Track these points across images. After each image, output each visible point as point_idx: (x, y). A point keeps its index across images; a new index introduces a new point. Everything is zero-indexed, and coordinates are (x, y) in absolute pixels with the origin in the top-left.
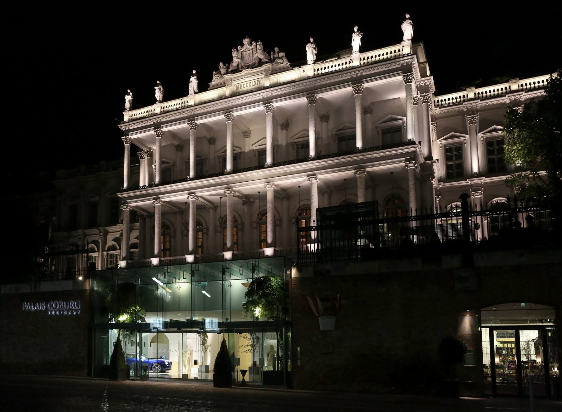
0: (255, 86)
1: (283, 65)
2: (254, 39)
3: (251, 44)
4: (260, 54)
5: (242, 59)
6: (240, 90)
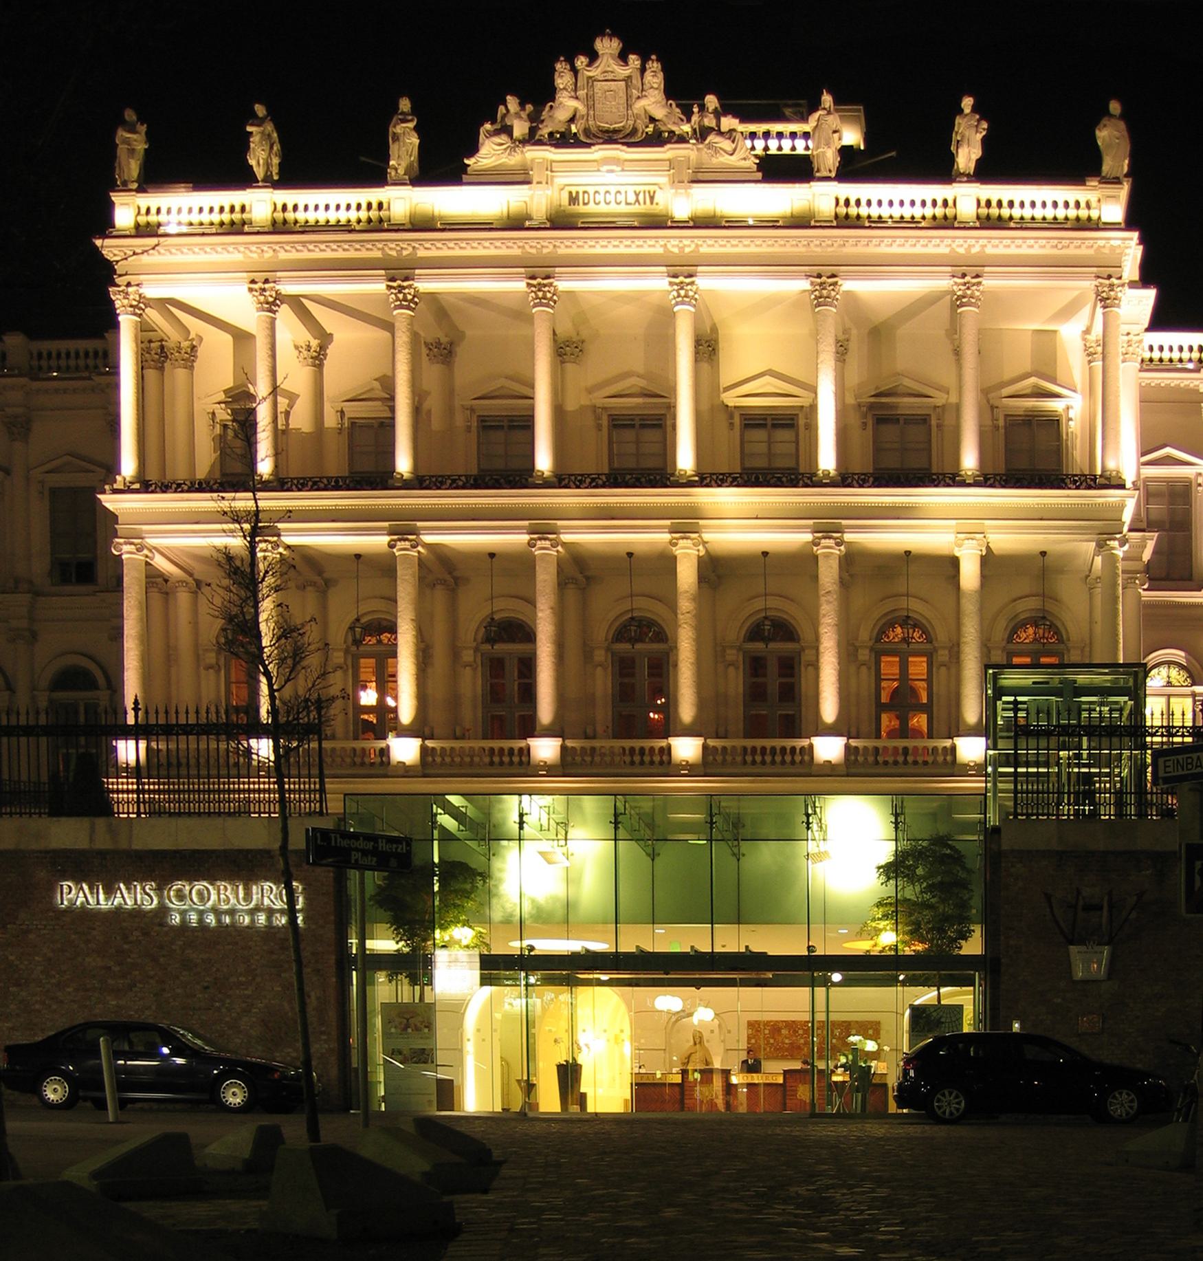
0: (636, 209)
1: (733, 161)
3: (623, 57)
4: (653, 102)
5: (590, 101)
6: (581, 208)
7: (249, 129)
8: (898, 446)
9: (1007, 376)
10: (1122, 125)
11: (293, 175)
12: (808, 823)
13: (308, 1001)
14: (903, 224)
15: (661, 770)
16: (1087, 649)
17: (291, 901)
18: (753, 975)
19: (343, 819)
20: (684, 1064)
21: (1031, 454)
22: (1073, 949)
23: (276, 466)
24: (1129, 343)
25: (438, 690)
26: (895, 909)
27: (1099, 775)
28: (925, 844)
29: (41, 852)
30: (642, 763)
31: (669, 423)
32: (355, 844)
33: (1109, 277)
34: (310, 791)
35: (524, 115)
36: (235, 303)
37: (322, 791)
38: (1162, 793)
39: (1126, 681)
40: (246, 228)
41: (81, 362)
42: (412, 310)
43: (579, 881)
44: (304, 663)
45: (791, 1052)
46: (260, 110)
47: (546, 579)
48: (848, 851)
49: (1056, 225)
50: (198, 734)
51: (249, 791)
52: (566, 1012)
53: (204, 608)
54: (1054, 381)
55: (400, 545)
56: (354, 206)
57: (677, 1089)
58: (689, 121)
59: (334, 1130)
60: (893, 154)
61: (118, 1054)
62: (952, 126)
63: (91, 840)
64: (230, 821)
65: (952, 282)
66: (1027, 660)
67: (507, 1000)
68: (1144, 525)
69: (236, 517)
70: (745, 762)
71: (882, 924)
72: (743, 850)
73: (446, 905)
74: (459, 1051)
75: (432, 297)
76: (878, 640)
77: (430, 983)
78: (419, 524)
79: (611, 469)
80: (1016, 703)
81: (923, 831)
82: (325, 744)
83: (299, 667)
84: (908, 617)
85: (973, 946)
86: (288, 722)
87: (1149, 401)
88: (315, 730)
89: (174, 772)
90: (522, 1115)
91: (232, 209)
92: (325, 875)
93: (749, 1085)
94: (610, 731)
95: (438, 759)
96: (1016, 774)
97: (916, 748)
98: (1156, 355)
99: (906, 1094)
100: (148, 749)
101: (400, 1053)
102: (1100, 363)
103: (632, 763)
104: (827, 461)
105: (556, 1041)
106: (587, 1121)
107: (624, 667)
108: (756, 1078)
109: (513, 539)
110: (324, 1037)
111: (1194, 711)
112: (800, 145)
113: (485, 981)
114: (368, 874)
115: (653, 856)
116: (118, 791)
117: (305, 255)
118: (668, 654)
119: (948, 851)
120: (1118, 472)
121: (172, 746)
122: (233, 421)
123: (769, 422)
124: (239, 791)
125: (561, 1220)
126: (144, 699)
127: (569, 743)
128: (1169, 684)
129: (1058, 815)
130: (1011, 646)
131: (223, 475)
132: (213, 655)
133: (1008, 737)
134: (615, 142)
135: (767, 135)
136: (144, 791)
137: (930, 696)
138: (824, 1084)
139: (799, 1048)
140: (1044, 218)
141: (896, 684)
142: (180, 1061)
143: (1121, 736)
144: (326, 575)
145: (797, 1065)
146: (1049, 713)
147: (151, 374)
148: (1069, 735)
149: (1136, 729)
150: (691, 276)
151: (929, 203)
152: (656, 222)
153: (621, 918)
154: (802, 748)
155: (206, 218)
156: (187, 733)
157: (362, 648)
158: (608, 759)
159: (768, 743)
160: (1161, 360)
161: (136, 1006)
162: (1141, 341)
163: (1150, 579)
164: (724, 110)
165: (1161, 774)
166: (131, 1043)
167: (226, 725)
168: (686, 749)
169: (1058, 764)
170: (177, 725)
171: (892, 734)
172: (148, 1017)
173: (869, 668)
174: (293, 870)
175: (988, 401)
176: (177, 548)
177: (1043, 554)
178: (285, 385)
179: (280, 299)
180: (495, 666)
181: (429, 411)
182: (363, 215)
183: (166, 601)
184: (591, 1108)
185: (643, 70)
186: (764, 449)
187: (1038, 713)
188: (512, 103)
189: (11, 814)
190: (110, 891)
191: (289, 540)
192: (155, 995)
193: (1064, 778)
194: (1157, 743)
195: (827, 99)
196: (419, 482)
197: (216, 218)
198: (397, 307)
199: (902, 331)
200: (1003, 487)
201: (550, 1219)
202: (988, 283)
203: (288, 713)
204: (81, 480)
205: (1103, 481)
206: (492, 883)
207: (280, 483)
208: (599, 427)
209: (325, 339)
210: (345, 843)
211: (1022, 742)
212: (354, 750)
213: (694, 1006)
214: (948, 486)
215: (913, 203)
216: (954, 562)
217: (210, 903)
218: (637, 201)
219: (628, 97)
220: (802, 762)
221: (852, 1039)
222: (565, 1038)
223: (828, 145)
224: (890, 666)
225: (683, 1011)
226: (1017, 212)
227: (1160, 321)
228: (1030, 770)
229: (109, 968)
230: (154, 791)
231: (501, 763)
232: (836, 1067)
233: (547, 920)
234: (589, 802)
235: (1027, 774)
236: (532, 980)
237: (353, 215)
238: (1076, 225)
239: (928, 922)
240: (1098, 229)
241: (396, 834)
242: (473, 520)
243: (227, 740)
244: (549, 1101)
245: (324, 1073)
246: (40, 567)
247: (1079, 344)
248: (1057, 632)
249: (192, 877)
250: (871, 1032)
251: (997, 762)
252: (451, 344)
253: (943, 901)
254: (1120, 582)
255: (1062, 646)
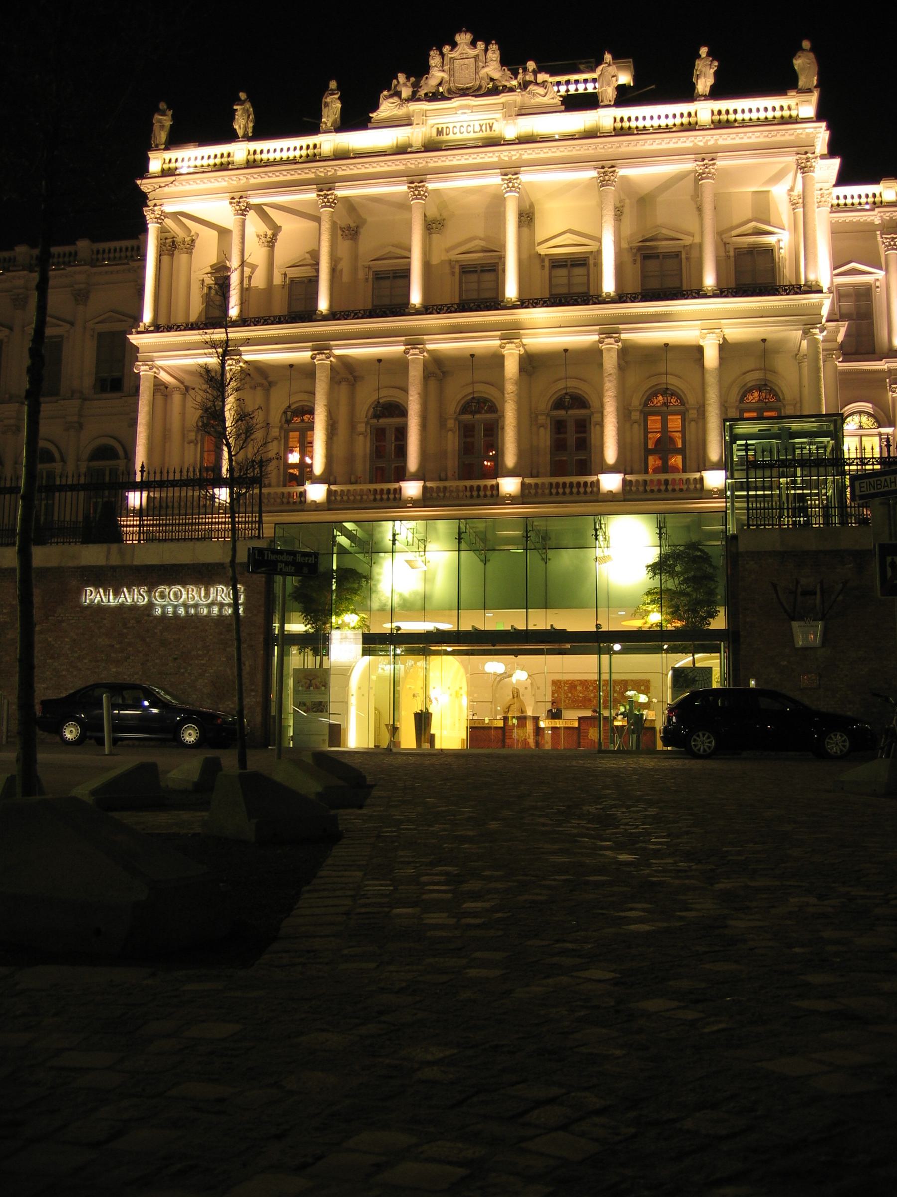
1: (545, 100)
2: (481, 36)
3: (473, 44)
4: (493, 69)
6: (444, 137)
7: (235, 107)
8: (660, 273)
9: (735, 222)
10: (811, 55)
11: (261, 132)
12: (596, 535)
13: (243, 668)
14: (659, 130)
15: (492, 501)
16: (799, 405)
17: (236, 598)
18: (556, 646)
19: (273, 540)
20: (505, 712)
21: (753, 272)
22: (795, 624)
23: (241, 311)
24: (822, 195)
25: (340, 451)
26: (660, 596)
27: (810, 495)
28: (681, 548)
29: (74, 568)
30: (479, 496)
31: (500, 268)
32: (280, 557)
33: (806, 153)
34: (252, 522)
35: (409, 84)
36: (221, 212)
37: (260, 522)
38: (859, 507)
39: (828, 427)
40: (230, 166)
41: (123, 254)
42: (333, 208)
43: (432, 580)
44: (253, 437)
45: (583, 703)
46: (243, 96)
47: (415, 375)
48: (625, 555)
49: (767, 122)
50: (181, 486)
51: (212, 523)
52: (421, 674)
53: (190, 404)
54: (768, 223)
55: (319, 357)
56: (298, 148)
57: (500, 731)
58: (516, 78)
59: (257, 761)
60: (653, 87)
61: (114, 706)
62: (693, 66)
63: (107, 559)
64: (198, 544)
65: (695, 164)
66: (755, 415)
67: (381, 666)
68: (837, 317)
69: (213, 345)
70: (551, 494)
71: (650, 608)
72: (549, 556)
73: (340, 599)
74: (346, 703)
75: (346, 199)
76: (646, 405)
77: (328, 654)
78: (332, 343)
79: (460, 300)
80: (747, 445)
81: (680, 539)
82: (264, 490)
83: (249, 440)
84: (667, 389)
85: (719, 623)
86: (240, 477)
87: (837, 233)
88: (257, 481)
89: (163, 512)
90: (389, 750)
91: (222, 156)
92: (259, 579)
93: (553, 728)
94: (457, 475)
95: (339, 498)
96: (748, 496)
97: (674, 480)
98: (842, 201)
99: (670, 735)
100: (148, 497)
101: (305, 704)
102: (802, 210)
103: (472, 496)
104: (609, 286)
105: (414, 696)
106: (435, 755)
107: (467, 431)
108: (558, 723)
109: (394, 349)
110: (253, 694)
111: (880, 446)
112: (590, 88)
113: (366, 652)
114: (288, 578)
115: (485, 561)
116: (127, 526)
117: (267, 179)
118: (497, 421)
119: (699, 553)
120: (817, 282)
121: (164, 495)
122: (215, 284)
123: (569, 263)
124: (205, 524)
125: (414, 829)
126: (148, 464)
127: (429, 484)
128: (861, 428)
129: (780, 525)
130: (742, 406)
131: (207, 318)
132: (194, 434)
133: (741, 470)
134: (468, 95)
135: (568, 82)
136: (143, 526)
137: (684, 443)
138: (608, 727)
139: (590, 700)
140: (759, 119)
141: (659, 435)
142: (155, 711)
143: (826, 466)
144: (270, 379)
145: (588, 713)
146: (771, 452)
147: (165, 259)
148: (787, 467)
149: (837, 461)
150: (516, 174)
151: (678, 115)
152: (494, 142)
153: (462, 606)
154: (592, 483)
155: (205, 162)
156: (174, 486)
157: (291, 426)
158: (455, 494)
159: (568, 480)
160: (845, 205)
161: (127, 673)
162: (830, 193)
163: (843, 354)
164: (540, 69)
165: (857, 493)
166: (123, 699)
167: (200, 479)
168: (509, 485)
169: (779, 488)
170: (168, 481)
171: (656, 471)
172: (136, 680)
173: (640, 425)
174: (238, 576)
175: (722, 240)
176: (174, 366)
177: (764, 340)
178: (249, 260)
179: (249, 207)
180: (379, 434)
181: (342, 270)
182: (304, 152)
183: (166, 401)
184: (438, 745)
185: (486, 50)
186: (565, 281)
187: (763, 452)
188: (401, 77)
189: (57, 543)
190: (117, 593)
191: (246, 357)
192: (142, 664)
193: (784, 498)
194: (853, 470)
195: (608, 57)
196: (334, 315)
197: (212, 161)
198: (323, 207)
199: (660, 199)
200: (734, 296)
201: (406, 829)
202: (719, 163)
203: (240, 470)
204: (117, 327)
205: (806, 289)
206: (373, 582)
207: (243, 321)
208: (453, 274)
209: (276, 229)
210: (273, 557)
211: (752, 473)
212: (283, 493)
213: (514, 669)
214: (695, 298)
215: (667, 116)
216: (700, 349)
217: (182, 600)
218: (481, 130)
219: (477, 67)
220: (591, 492)
221: (629, 693)
222: (420, 693)
223: (609, 85)
224: (654, 423)
225: (505, 673)
226: (739, 117)
227: (843, 179)
228: (759, 493)
229: (113, 646)
230: (150, 525)
231: (382, 499)
232: (617, 715)
233: (410, 608)
234: (441, 525)
235: (756, 496)
236: (398, 651)
237: (298, 153)
238: (781, 121)
239: (685, 606)
240: (797, 122)
241: (308, 550)
242: (368, 338)
243: (200, 490)
244: (408, 740)
245: (252, 720)
246: (88, 382)
247: (786, 198)
248: (776, 394)
249: (171, 583)
250: (643, 688)
251: (733, 488)
252: (357, 227)
253: (695, 590)
254: (821, 357)
255: (780, 404)
